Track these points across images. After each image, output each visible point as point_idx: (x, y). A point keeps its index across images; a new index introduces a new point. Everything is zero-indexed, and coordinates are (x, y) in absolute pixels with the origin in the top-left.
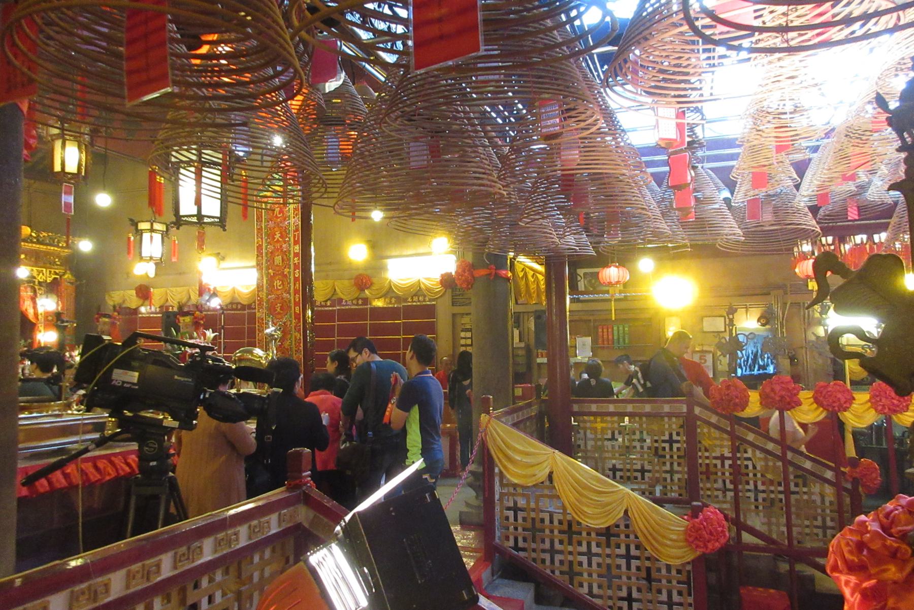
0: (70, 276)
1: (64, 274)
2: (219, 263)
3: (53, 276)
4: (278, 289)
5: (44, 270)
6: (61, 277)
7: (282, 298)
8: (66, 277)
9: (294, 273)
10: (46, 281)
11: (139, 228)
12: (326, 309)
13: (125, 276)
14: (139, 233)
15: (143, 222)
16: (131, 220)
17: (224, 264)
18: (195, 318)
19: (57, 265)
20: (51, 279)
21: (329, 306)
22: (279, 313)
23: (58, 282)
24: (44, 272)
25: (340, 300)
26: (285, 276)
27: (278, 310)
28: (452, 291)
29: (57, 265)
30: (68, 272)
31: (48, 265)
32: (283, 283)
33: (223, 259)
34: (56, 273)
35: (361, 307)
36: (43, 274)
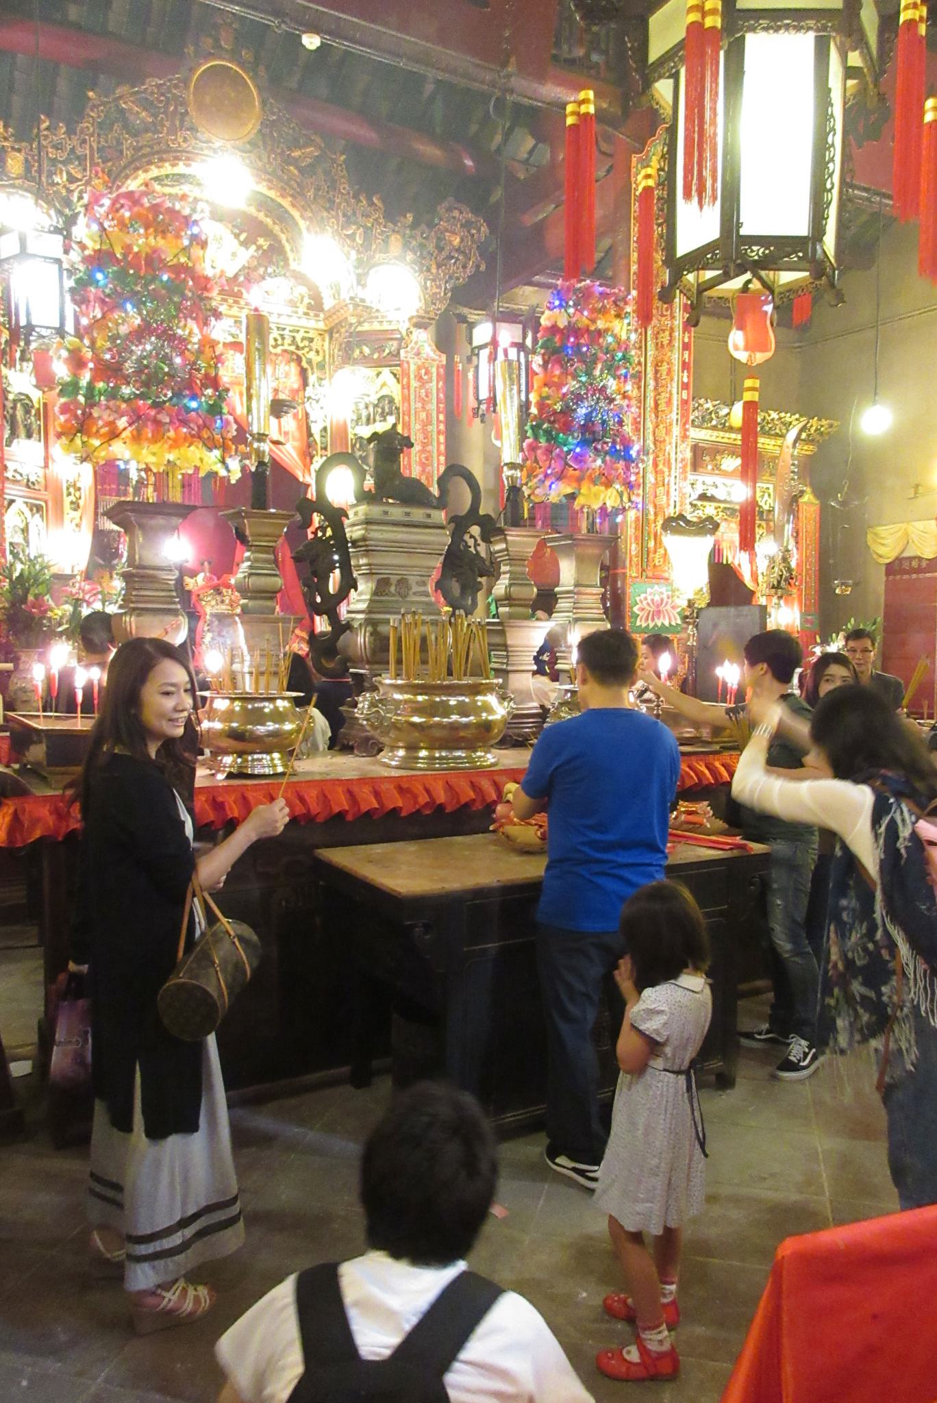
36: (769, 495)
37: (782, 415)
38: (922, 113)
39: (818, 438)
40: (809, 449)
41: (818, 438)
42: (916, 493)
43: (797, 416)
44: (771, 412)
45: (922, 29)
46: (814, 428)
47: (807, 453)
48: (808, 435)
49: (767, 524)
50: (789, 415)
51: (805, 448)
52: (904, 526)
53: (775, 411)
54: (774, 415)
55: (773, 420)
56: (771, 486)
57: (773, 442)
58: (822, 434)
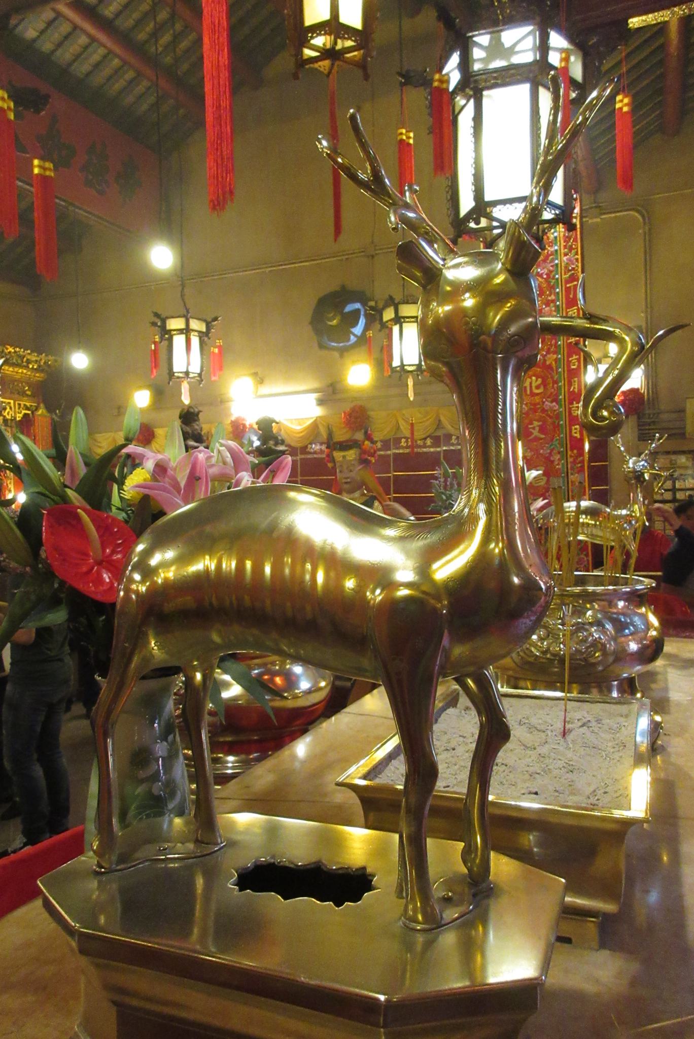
0: (44, 411)
1: (37, 408)
2: (257, 388)
3: (24, 412)
4: (533, 394)
5: (12, 402)
6: (33, 413)
7: (544, 411)
8: (40, 412)
9: (569, 362)
10: (15, 418)
11: (168, 328)
12: (425, 450)
13: (115, 412)
14: (167, 335)
15: (173, 317)
16: (157, 315)
17: (265, 389)
18: (364, 452)
19: (27, 395)
20: (21, 415)
21: (429, 447)
22: (537, 439)
23: (30, 421)
24: (12, 405)
25: (448, 437)
26: (550, 367)
27: (536, 433)
28: (639, 418)
29: (27, 395)
30: (42, 405)
31: (16, 396)
32: (544, 384)
33: (261, 381)
34: (27, 408)
35: (432, 450)
36: (11, 408)
37: (18, 349)
38: (32, 166)
39: (46, 368)
40: (39, 376)
41: (46, 368)
42: (119, 412)
43: (29, 351)
44: (8, 347)
45: (11, 116)
46: (43, 361)
47: (39, 379)
48: (39, 366)
49: (11, 430)
50: (22, 350)
51: (37, 375)
52: (112, 434)
53: (11, 347)
54: (11, 349)
55: (10, 352)
56: (12, 402)
57: (11, 369)
58: (49, 366)
